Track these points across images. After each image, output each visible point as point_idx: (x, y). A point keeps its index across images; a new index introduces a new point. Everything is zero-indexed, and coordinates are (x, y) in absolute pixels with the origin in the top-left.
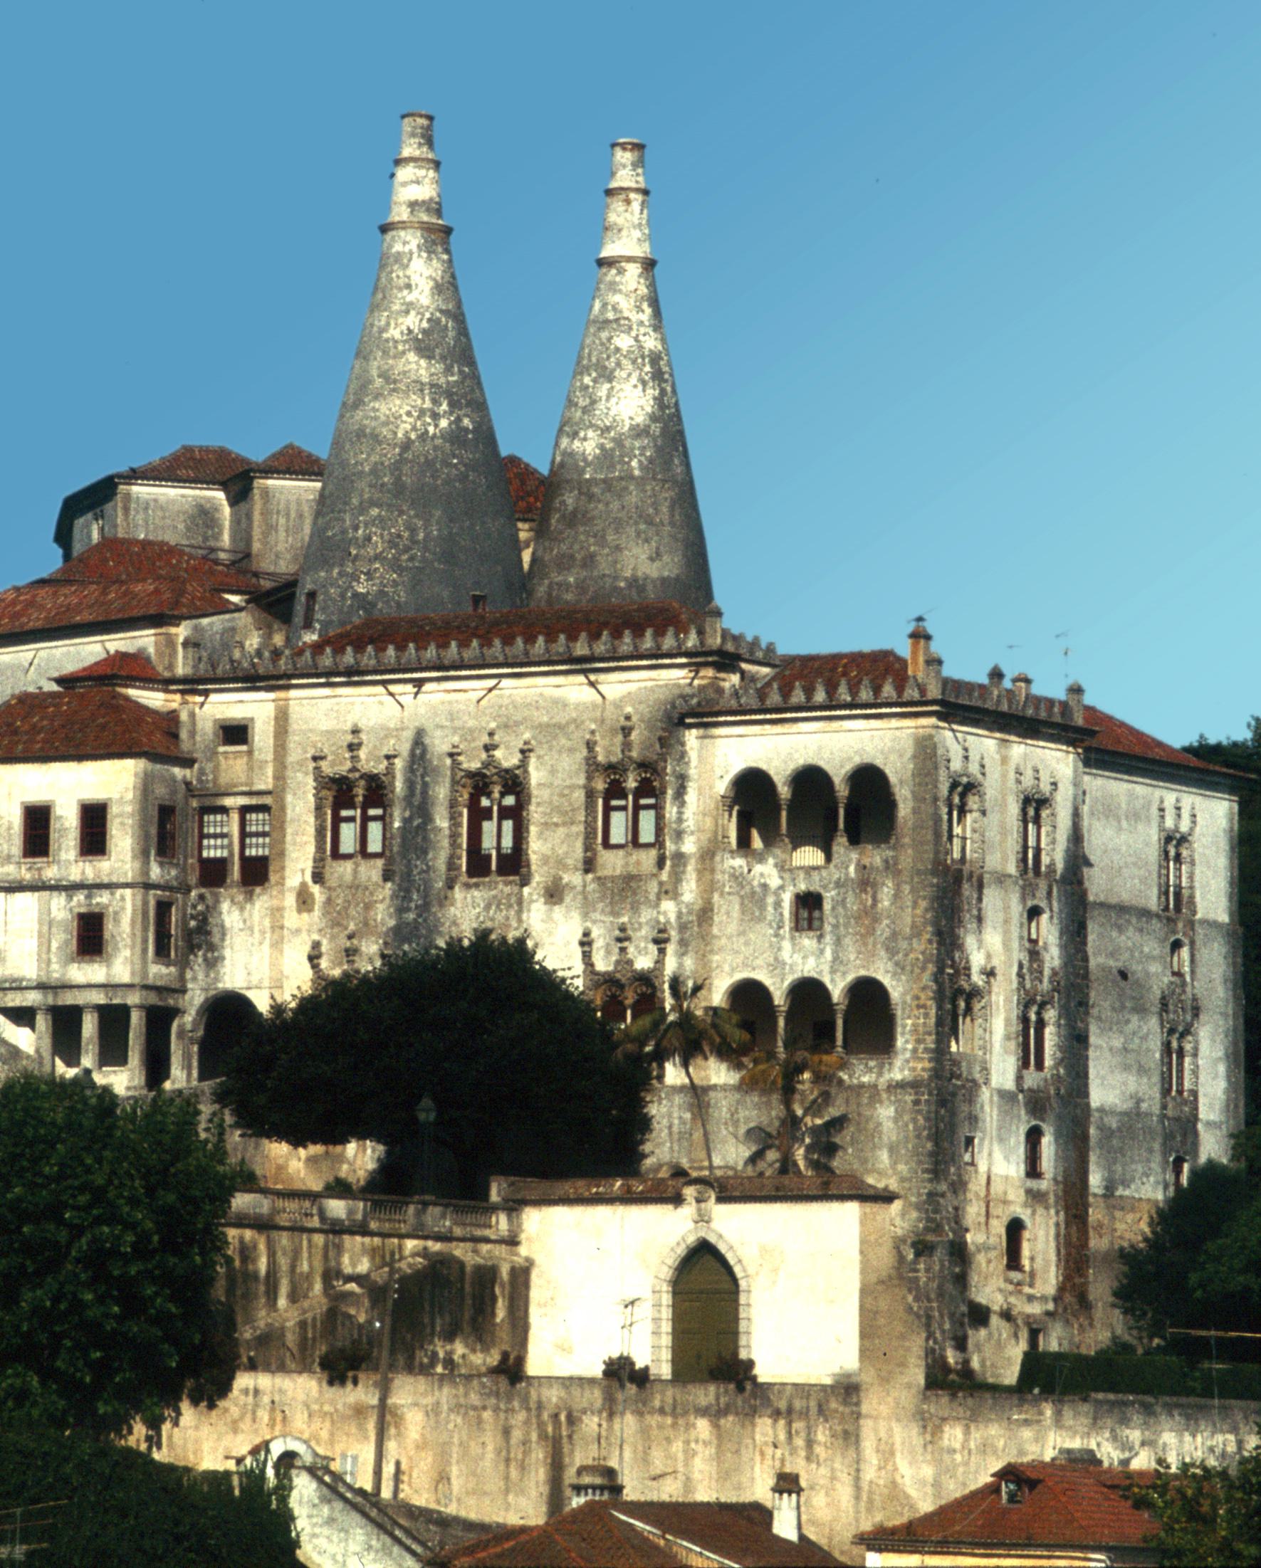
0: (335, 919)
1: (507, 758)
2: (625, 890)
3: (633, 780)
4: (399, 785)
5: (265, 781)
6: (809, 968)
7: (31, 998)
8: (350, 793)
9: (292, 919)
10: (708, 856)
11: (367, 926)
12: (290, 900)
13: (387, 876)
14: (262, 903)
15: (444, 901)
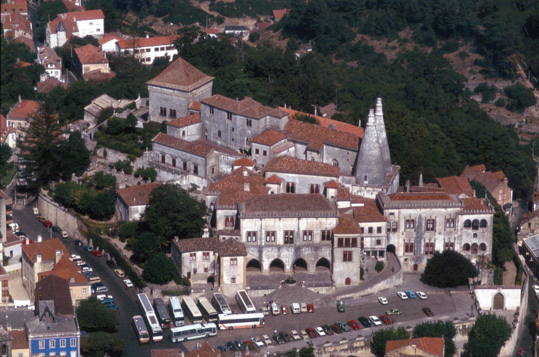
0: (407, 236)
1: (433, 218)
2: (450, 233)
3: (451, 221)
4: (417, 220)
5: (397, 219)
6: (475, 242)
7: (370, 250)
8: (409, 221)
9: (401, 236)
10: (461, 230)
11: (412, 237)
12: (401, 234)
13: (415, 231)
14: (396, 234)
15: (424, 234)
